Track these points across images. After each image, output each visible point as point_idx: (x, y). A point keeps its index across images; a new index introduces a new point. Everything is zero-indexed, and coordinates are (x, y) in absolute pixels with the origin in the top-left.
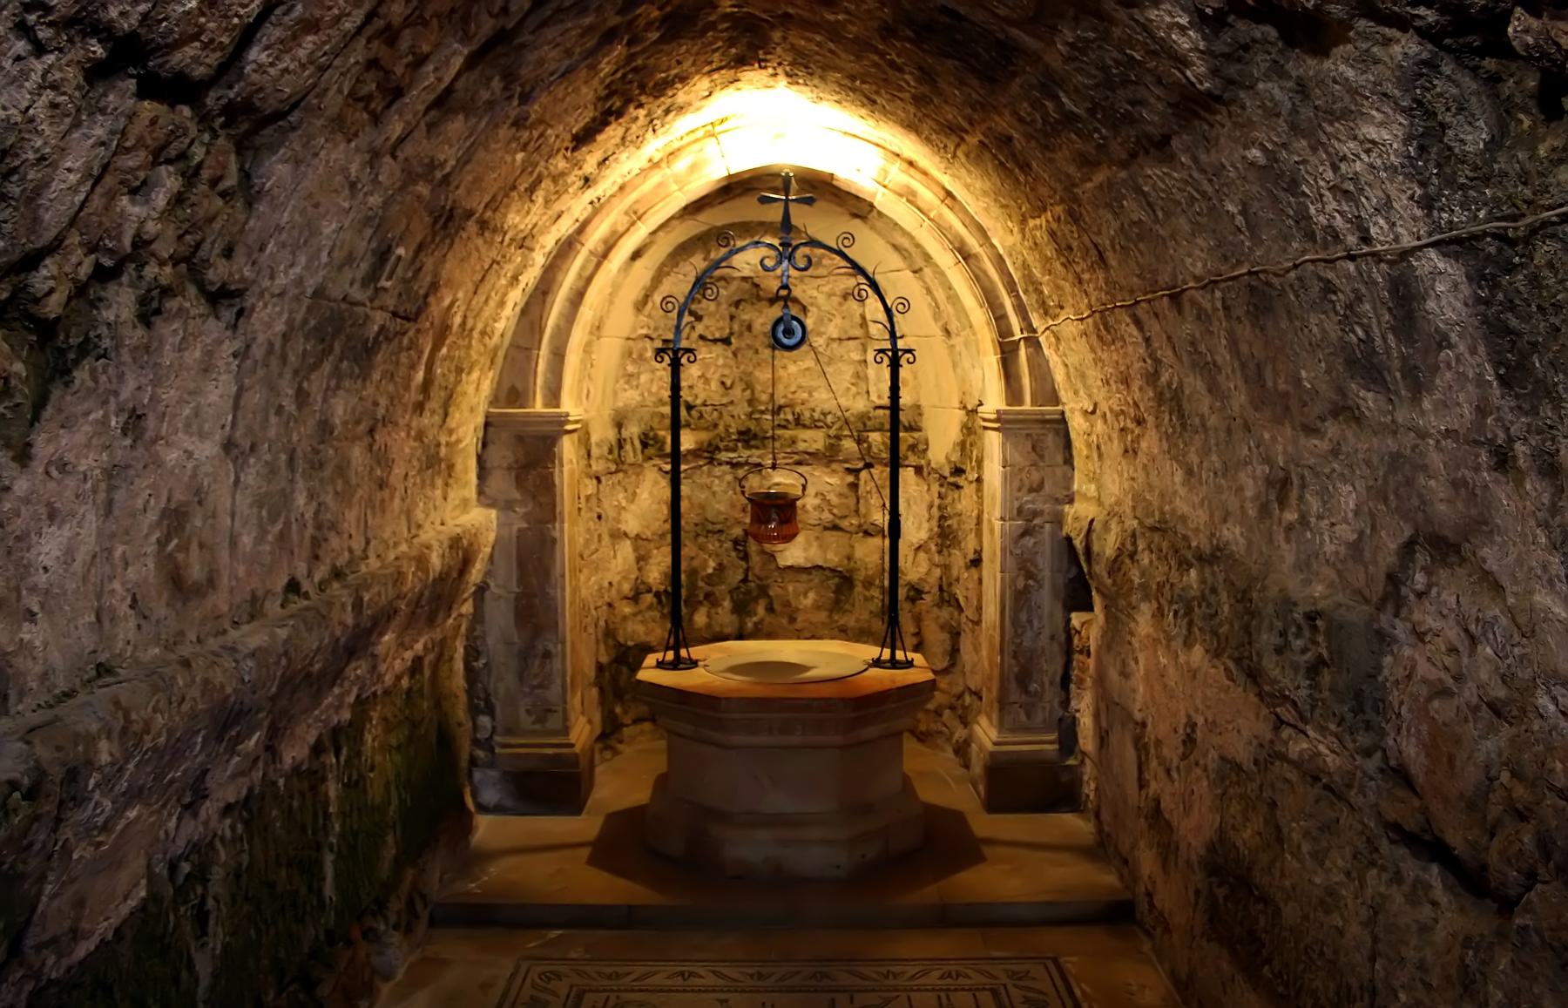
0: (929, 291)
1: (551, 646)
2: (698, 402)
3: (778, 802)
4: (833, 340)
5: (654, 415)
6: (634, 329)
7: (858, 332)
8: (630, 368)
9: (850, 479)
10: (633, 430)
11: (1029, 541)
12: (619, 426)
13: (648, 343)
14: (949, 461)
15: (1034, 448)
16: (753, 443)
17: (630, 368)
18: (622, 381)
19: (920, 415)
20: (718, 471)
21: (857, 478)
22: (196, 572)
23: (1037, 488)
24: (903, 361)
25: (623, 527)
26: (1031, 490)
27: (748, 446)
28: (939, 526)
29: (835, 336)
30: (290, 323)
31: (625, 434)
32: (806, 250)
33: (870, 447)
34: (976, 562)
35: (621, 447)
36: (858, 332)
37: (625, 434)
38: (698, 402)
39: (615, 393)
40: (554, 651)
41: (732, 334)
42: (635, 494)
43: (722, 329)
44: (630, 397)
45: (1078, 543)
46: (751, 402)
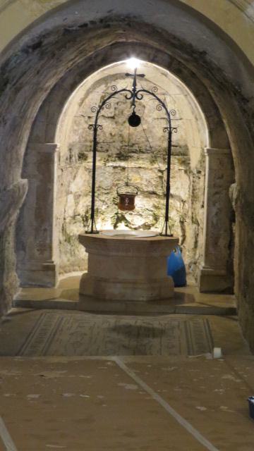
0: (190, 103)
1: (46, 227)
2: (101, 141)
4: (155, 119)
5: (83, 146)
6: (77, 113)
8: (76, 128)
9: (160, 174)
10: (76, 152)
11: (218, 196)
12: (70, 150)
13: (82, 118)
14: (196, 168)
15: (220, 163)
16: (122, 158)
17: (76, 128)
19: (188, 149)
20: (108, 169)
23: (222, 177)
24: (173, 132)
26: (219, 178)
28: (193, 193)
29: (156, 117)
32: (140, 93)
34: (203, 206)
35: (71, 158)
37: (73, 153)
38: (101, 141)
40: (48, 228)
41: (115, 115)
42: (75, 177)
43: (111, 113)
44: (76, 138)
45: (230, 196)
46: (122, 142)
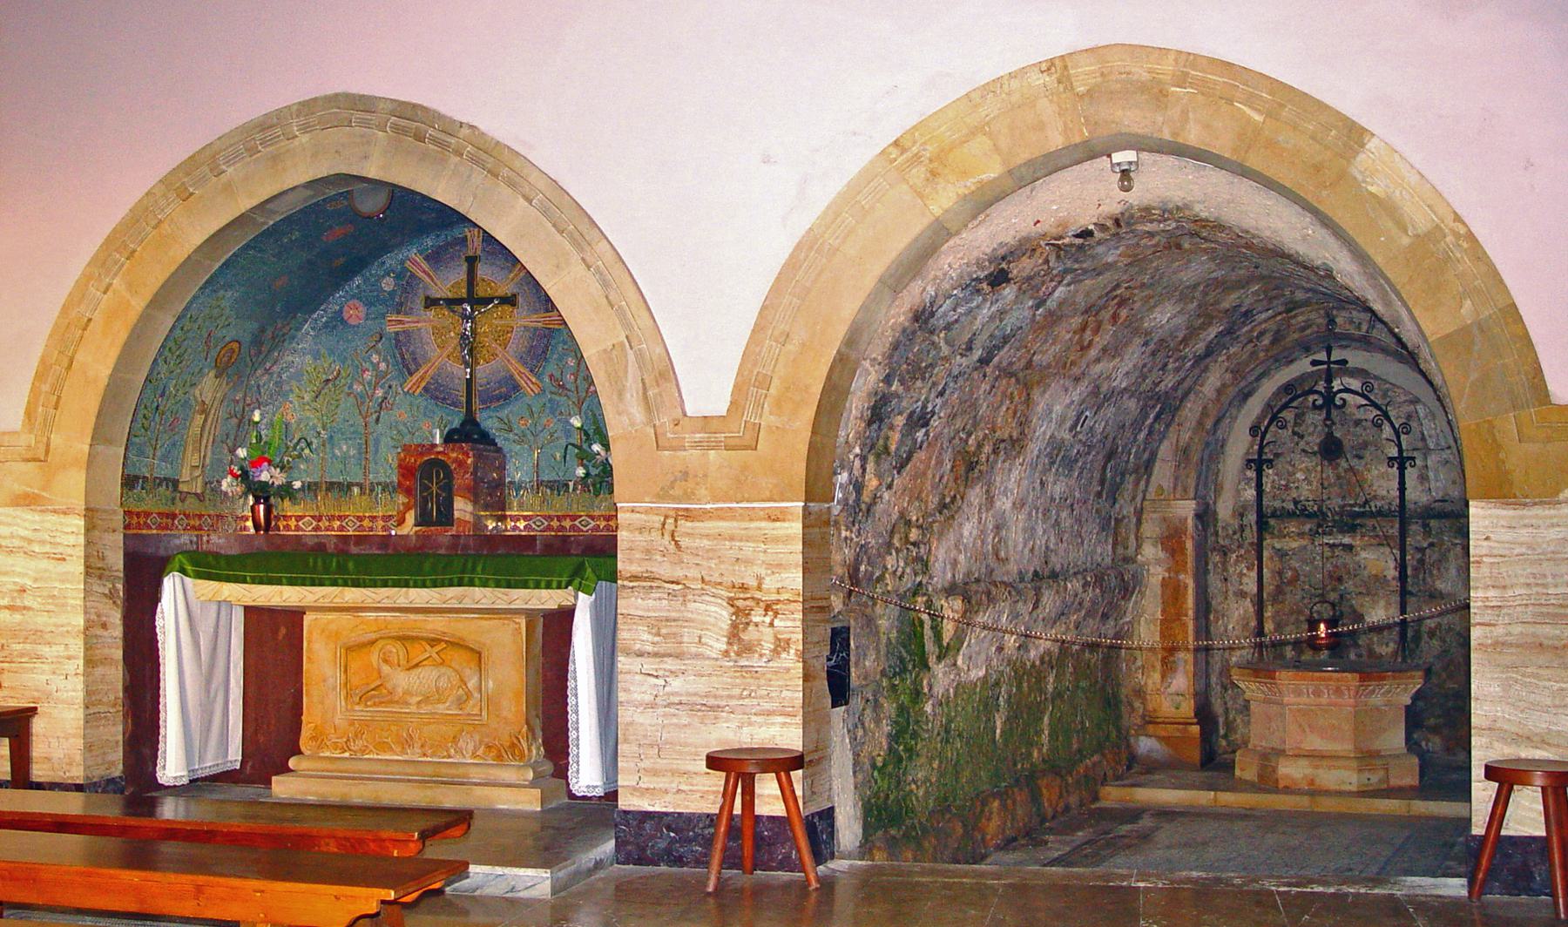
3: (1315, 742)
7: (1420, 445)
9: (1419, 556)
18: (1243, 483)
21: (1424, 555)
22: (1002, 554)
25: (1245, 589)
27: (1342, 531)
30: (1040, 450)
31: (1245, 521)
32: (1344, 395)
33: (1431, 530)
36: (1420, 445)
37: (1245, 521)
38: (1302, 498)
39: (1238, 492)
